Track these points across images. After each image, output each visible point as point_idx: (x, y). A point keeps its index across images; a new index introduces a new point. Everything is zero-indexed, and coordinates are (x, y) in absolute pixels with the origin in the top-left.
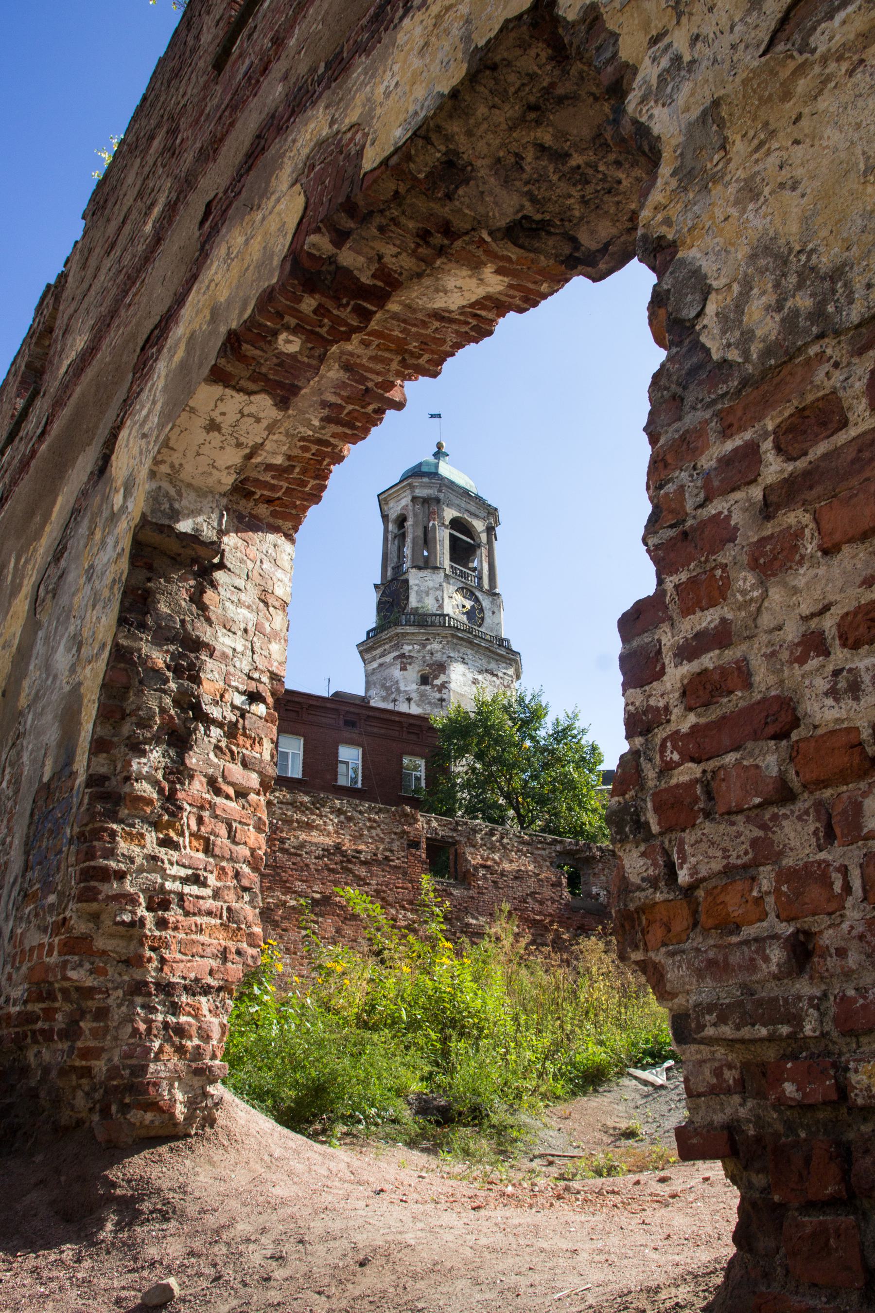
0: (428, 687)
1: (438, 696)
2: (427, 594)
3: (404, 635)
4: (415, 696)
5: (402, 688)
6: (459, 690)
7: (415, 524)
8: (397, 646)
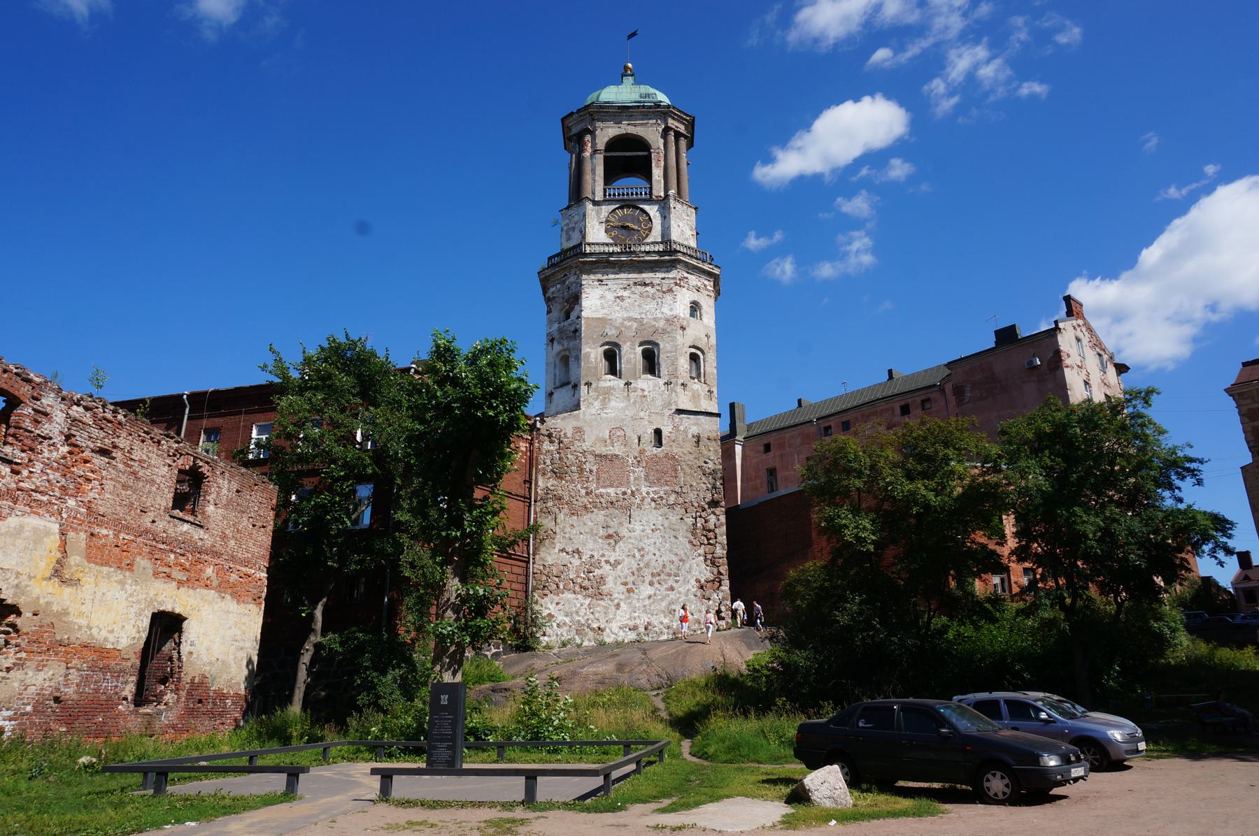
6: (595, 315)
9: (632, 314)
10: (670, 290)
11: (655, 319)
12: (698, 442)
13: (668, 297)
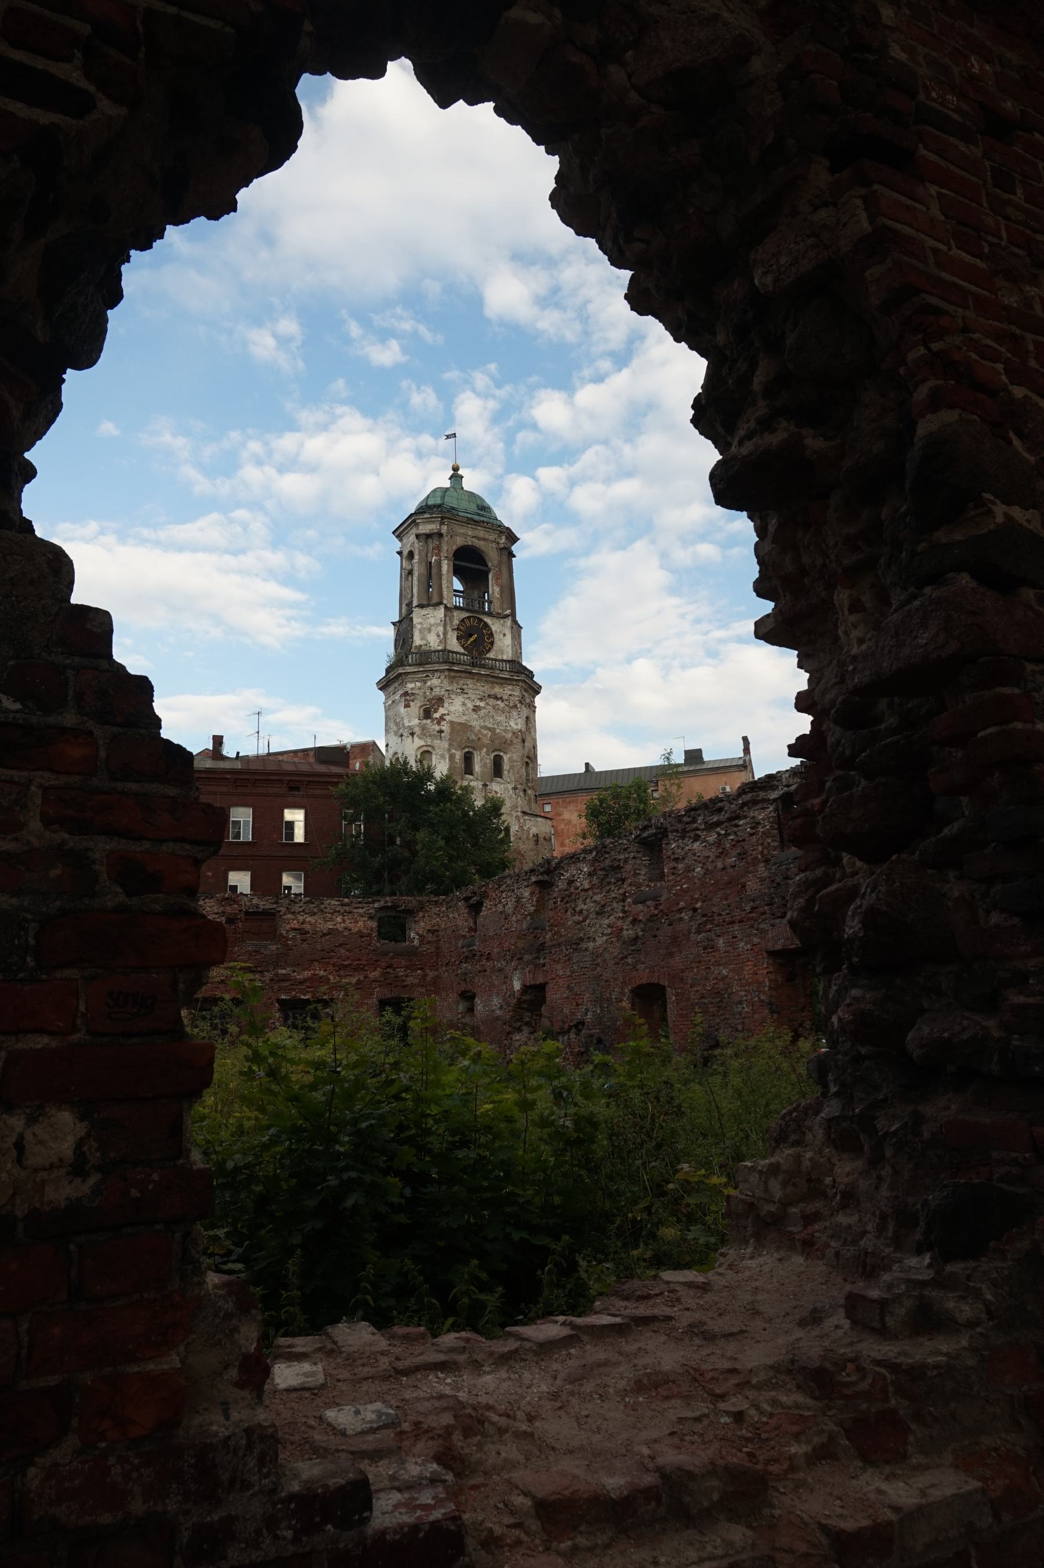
0: (429, 721)
1: (437, 728)
2: (430, 630)
4: (417, 730)
5: (407, 724)
7: (420, 563)
10: (515, 706)
11: (505, 731)
12: (537, 841)
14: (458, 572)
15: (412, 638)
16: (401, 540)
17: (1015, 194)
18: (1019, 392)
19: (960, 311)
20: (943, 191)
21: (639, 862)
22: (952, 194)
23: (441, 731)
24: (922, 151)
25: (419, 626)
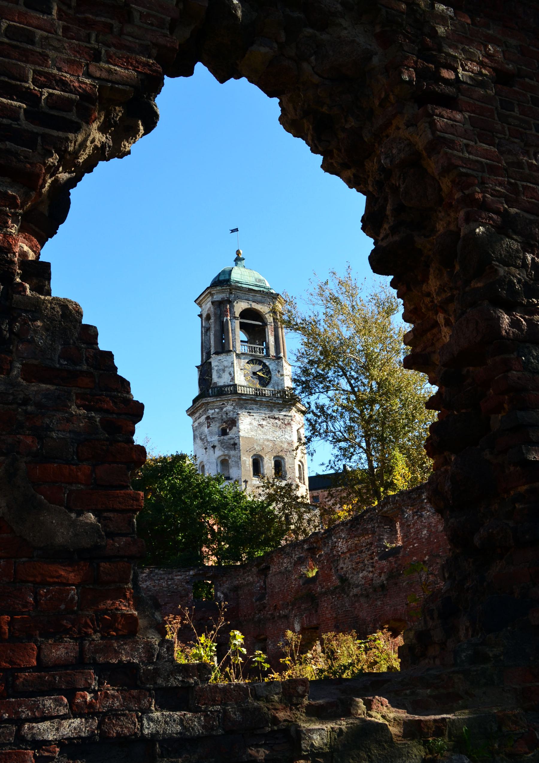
2: (224, 371)
3: (208, 403)
4: (216, 443)
6: (247, 435)
8: (206, 411)
9: (268, 437)
11: (282, 442)
13: (288, 428)
14: (243, 326)
15: (211, 377)
16: (201, 306)
17: (514, 111)
18: (513, 210)
19: (480, 174)
20: (472, 115)
21: (382, 529)
22: (477, 116)
23: (235, 444)
24: (461, 97)
25: (216, 368)
